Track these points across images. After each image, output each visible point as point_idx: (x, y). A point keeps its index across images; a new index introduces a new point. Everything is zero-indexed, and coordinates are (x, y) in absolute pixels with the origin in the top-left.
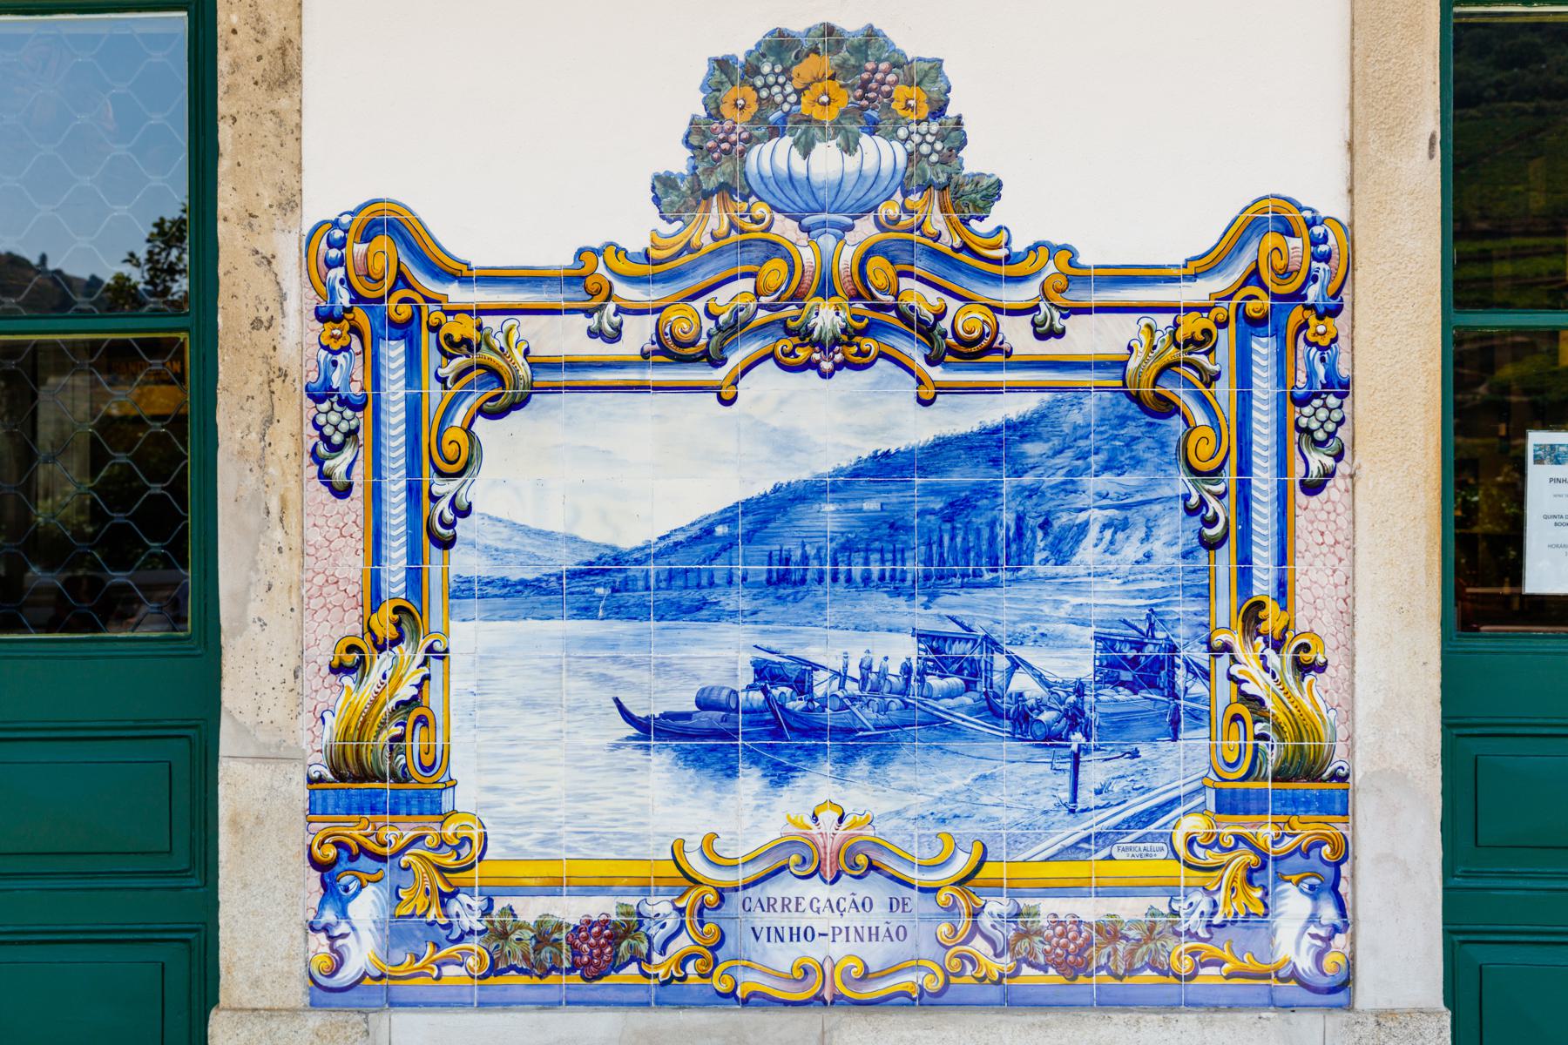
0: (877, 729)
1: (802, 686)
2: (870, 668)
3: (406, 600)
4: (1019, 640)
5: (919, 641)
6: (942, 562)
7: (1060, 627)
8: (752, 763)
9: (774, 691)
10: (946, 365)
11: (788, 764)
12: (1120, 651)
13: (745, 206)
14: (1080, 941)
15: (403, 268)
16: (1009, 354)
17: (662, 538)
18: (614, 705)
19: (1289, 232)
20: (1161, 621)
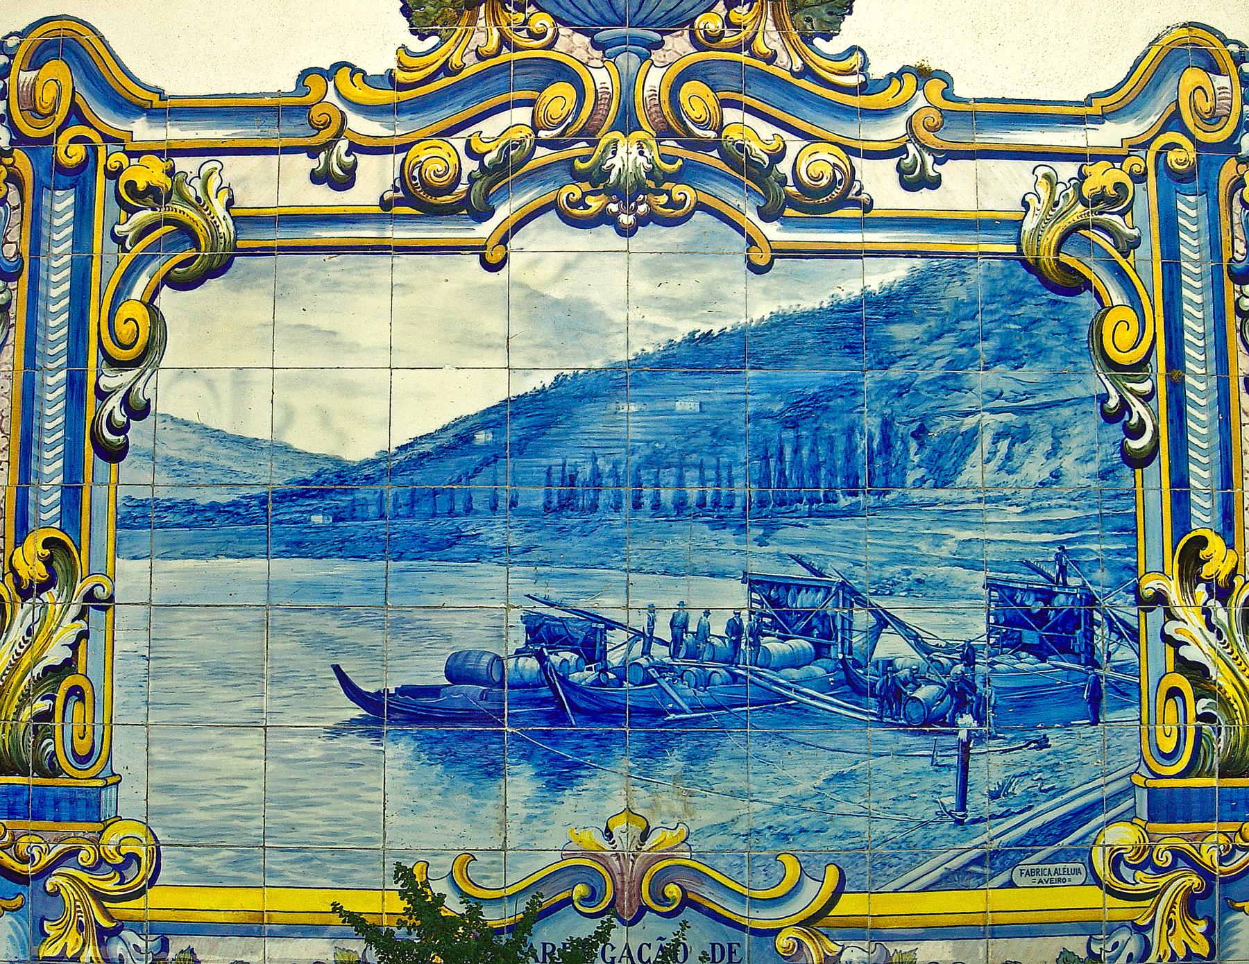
1: (591, 651)
2: (685, 626)
3: (60, 529)
4: (887, 588)
5: (752, 590)
6: (783, 481)
8: (522, 757)
9: (552, 657)
10: (786, 222)
11: (571, 758)
12: (1022, 604)
13: (521, 17)
15: (78, 100)
16: (868, 207)
17: (402, 448)
19: (1213, 68)
20: (1075, 563)
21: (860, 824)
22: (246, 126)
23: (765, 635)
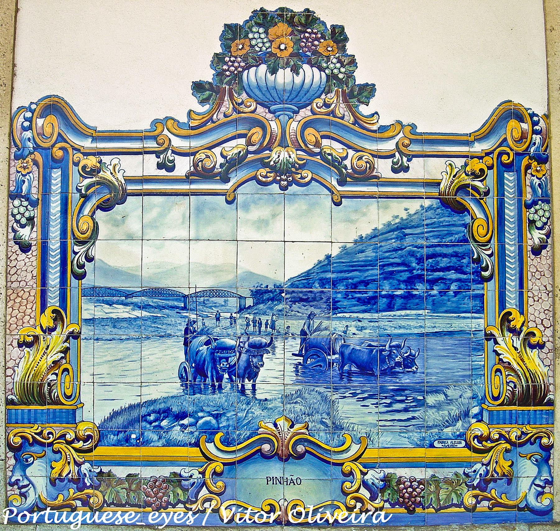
19: (521, 119)
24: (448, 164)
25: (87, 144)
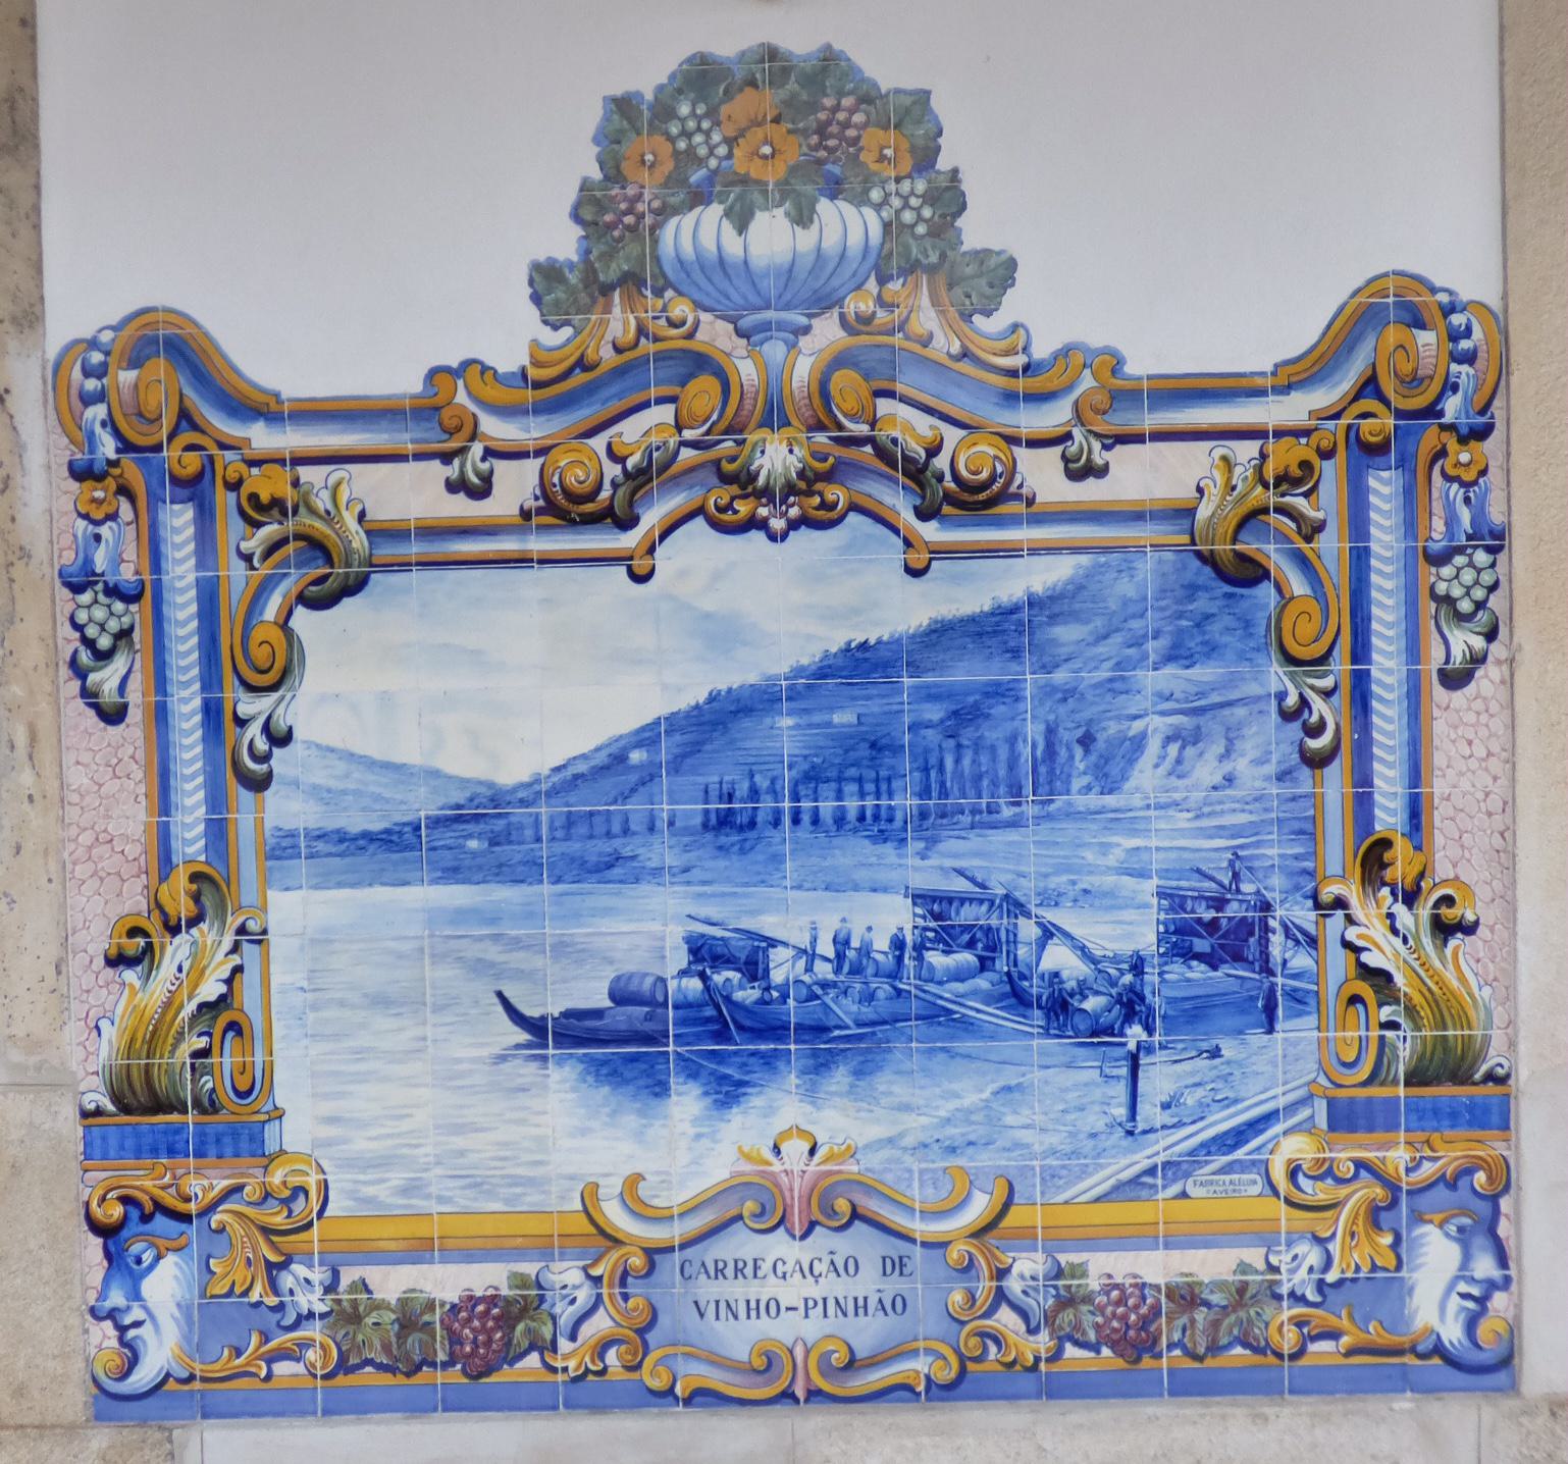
0: (859, 1025)
1: (754, 968)
2: (847, 942)
4: (1052, 900)
7: (1110, 880)
8: (689, 1076)
9: (716, 977)
13: (660, 303)
14: (1144, 1310)
15: (187, 403)
16: (1030, 502)
17: (557, 769)
18: (496, 1000)
20: (1250, 869)
21: (1026, 1136)
22: (372, 431)
23: (928, 949)
24: (1217, 458)
25: (262, 437)
